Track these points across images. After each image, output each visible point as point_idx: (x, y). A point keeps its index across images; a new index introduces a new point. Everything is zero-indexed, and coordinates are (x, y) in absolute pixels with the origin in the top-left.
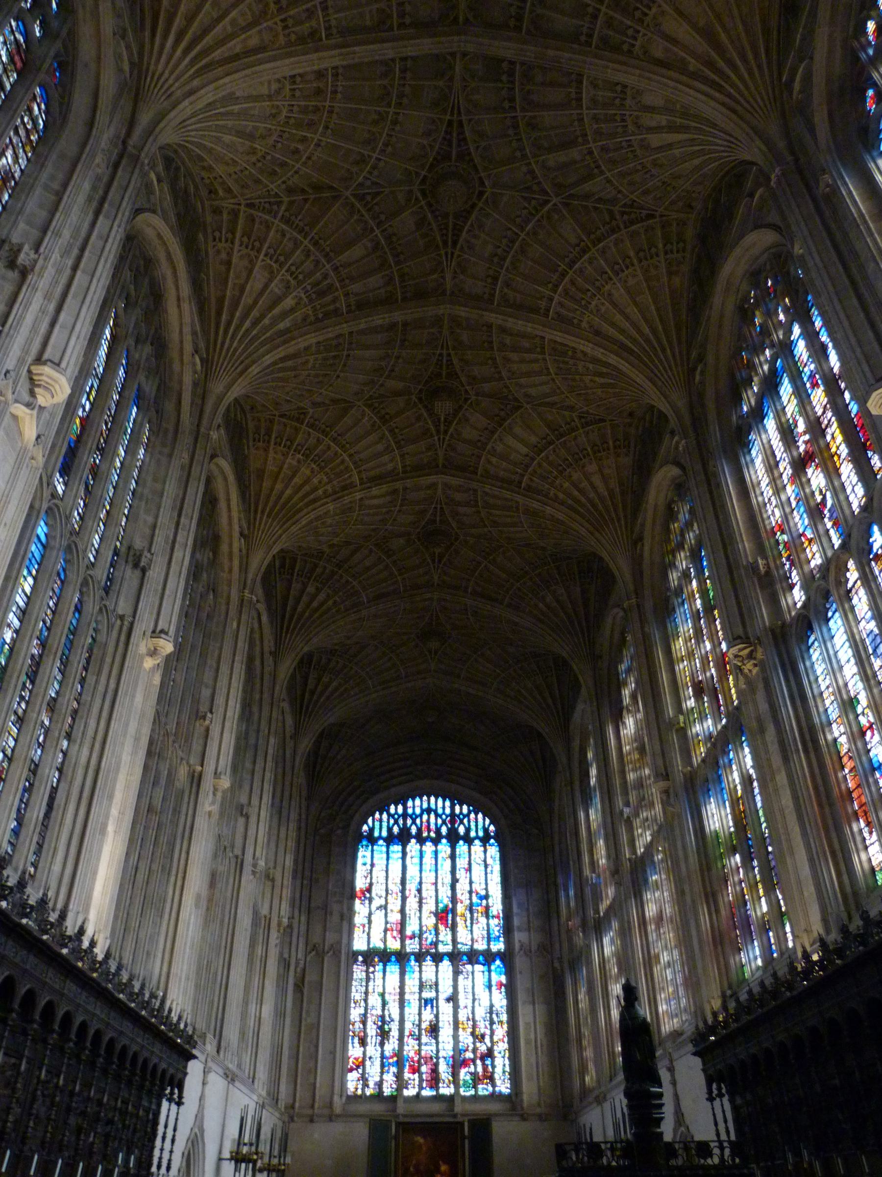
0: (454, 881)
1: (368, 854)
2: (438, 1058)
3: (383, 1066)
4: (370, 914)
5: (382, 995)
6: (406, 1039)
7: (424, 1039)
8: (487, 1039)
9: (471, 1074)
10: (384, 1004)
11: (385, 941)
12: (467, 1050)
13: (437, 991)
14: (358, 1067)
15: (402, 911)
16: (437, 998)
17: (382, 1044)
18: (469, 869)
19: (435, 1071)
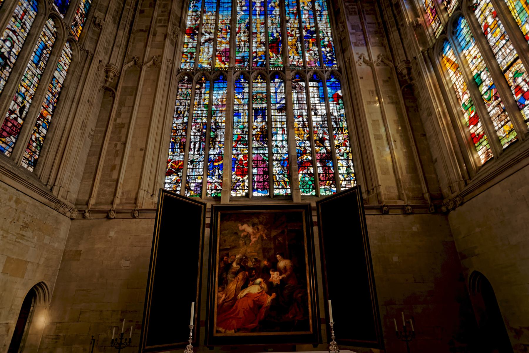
0: (283, 22)
1: (199, 5)
2: (271, 160)
3: (207, 168)
4: (199, 44)
5: (208, 107)
6: (234, 144)
7: (255, 144)
8: (327, 144)
9: (311, 175)
10: (210, 114)
11: (212, 63)
12: (305, 153)
13: (269, 103)
14: (178, 170)
15: (231, 42)
16: (269, 108)
17: (206, 149)
18: (298, 13)
19: (268, 173)
